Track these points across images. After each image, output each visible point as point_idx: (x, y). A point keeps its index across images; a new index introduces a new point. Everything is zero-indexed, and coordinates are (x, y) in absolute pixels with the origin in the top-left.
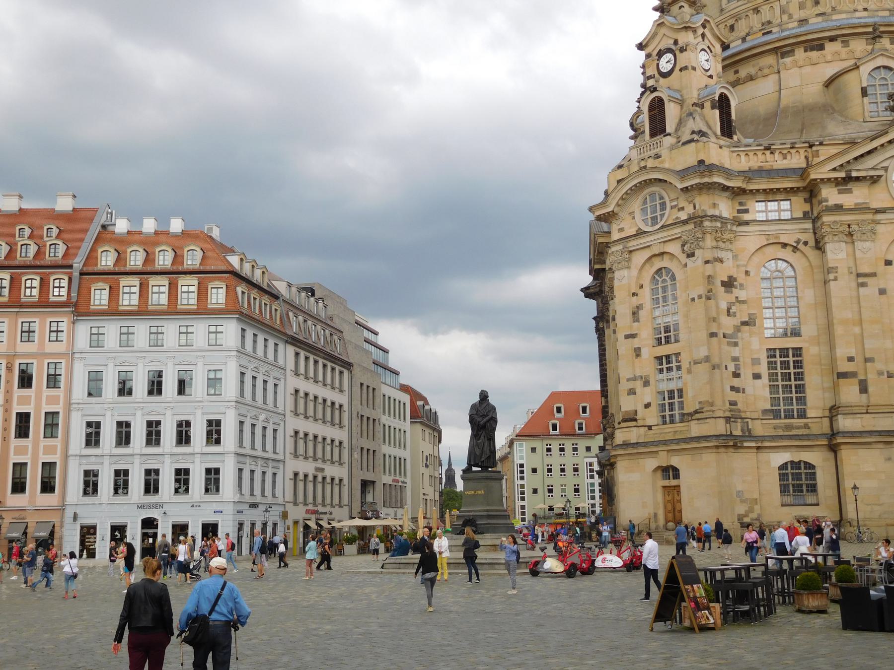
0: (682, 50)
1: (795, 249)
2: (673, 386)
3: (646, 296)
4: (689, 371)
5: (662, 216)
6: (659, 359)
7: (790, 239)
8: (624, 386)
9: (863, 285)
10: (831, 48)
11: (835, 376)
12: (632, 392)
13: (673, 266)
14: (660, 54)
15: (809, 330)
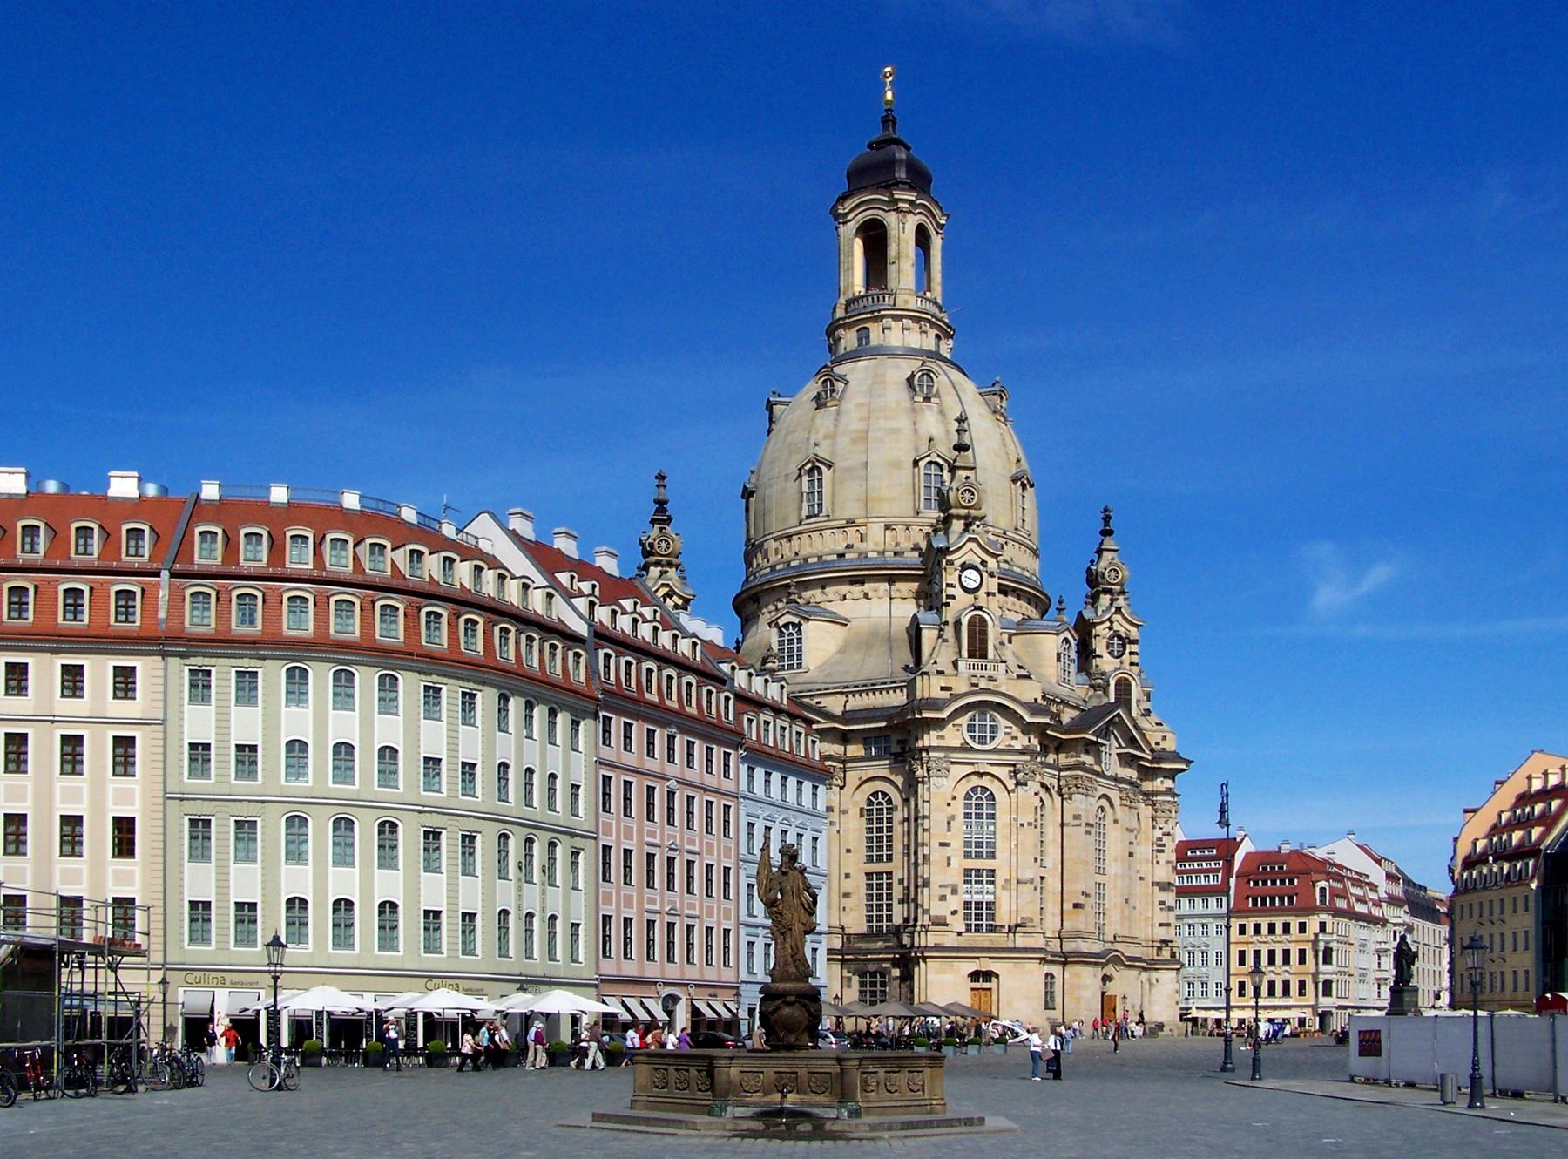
0: (991, 575)
1: (1048, 789)
2: (978, 898)
3: (959, 808)
4: (1003, 888)
5: (992, 738)
6: (967, 872)
7: (1047, 781)
8: (935, 890)
9: (1088, 833)
10: (1011, 599)
11: (1068, 906)
12: (943, 898)
13: (995, 787)
14: (964, 567)
15: (1048, 862)
